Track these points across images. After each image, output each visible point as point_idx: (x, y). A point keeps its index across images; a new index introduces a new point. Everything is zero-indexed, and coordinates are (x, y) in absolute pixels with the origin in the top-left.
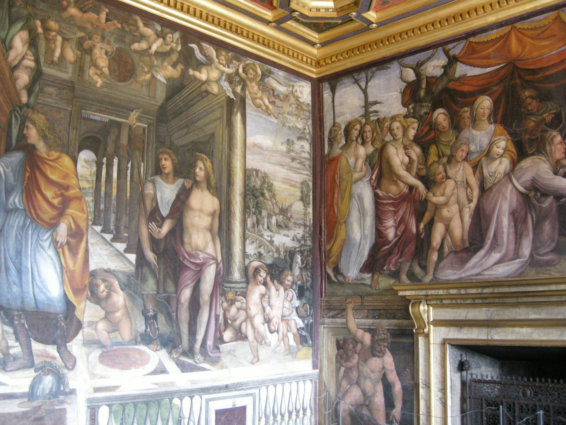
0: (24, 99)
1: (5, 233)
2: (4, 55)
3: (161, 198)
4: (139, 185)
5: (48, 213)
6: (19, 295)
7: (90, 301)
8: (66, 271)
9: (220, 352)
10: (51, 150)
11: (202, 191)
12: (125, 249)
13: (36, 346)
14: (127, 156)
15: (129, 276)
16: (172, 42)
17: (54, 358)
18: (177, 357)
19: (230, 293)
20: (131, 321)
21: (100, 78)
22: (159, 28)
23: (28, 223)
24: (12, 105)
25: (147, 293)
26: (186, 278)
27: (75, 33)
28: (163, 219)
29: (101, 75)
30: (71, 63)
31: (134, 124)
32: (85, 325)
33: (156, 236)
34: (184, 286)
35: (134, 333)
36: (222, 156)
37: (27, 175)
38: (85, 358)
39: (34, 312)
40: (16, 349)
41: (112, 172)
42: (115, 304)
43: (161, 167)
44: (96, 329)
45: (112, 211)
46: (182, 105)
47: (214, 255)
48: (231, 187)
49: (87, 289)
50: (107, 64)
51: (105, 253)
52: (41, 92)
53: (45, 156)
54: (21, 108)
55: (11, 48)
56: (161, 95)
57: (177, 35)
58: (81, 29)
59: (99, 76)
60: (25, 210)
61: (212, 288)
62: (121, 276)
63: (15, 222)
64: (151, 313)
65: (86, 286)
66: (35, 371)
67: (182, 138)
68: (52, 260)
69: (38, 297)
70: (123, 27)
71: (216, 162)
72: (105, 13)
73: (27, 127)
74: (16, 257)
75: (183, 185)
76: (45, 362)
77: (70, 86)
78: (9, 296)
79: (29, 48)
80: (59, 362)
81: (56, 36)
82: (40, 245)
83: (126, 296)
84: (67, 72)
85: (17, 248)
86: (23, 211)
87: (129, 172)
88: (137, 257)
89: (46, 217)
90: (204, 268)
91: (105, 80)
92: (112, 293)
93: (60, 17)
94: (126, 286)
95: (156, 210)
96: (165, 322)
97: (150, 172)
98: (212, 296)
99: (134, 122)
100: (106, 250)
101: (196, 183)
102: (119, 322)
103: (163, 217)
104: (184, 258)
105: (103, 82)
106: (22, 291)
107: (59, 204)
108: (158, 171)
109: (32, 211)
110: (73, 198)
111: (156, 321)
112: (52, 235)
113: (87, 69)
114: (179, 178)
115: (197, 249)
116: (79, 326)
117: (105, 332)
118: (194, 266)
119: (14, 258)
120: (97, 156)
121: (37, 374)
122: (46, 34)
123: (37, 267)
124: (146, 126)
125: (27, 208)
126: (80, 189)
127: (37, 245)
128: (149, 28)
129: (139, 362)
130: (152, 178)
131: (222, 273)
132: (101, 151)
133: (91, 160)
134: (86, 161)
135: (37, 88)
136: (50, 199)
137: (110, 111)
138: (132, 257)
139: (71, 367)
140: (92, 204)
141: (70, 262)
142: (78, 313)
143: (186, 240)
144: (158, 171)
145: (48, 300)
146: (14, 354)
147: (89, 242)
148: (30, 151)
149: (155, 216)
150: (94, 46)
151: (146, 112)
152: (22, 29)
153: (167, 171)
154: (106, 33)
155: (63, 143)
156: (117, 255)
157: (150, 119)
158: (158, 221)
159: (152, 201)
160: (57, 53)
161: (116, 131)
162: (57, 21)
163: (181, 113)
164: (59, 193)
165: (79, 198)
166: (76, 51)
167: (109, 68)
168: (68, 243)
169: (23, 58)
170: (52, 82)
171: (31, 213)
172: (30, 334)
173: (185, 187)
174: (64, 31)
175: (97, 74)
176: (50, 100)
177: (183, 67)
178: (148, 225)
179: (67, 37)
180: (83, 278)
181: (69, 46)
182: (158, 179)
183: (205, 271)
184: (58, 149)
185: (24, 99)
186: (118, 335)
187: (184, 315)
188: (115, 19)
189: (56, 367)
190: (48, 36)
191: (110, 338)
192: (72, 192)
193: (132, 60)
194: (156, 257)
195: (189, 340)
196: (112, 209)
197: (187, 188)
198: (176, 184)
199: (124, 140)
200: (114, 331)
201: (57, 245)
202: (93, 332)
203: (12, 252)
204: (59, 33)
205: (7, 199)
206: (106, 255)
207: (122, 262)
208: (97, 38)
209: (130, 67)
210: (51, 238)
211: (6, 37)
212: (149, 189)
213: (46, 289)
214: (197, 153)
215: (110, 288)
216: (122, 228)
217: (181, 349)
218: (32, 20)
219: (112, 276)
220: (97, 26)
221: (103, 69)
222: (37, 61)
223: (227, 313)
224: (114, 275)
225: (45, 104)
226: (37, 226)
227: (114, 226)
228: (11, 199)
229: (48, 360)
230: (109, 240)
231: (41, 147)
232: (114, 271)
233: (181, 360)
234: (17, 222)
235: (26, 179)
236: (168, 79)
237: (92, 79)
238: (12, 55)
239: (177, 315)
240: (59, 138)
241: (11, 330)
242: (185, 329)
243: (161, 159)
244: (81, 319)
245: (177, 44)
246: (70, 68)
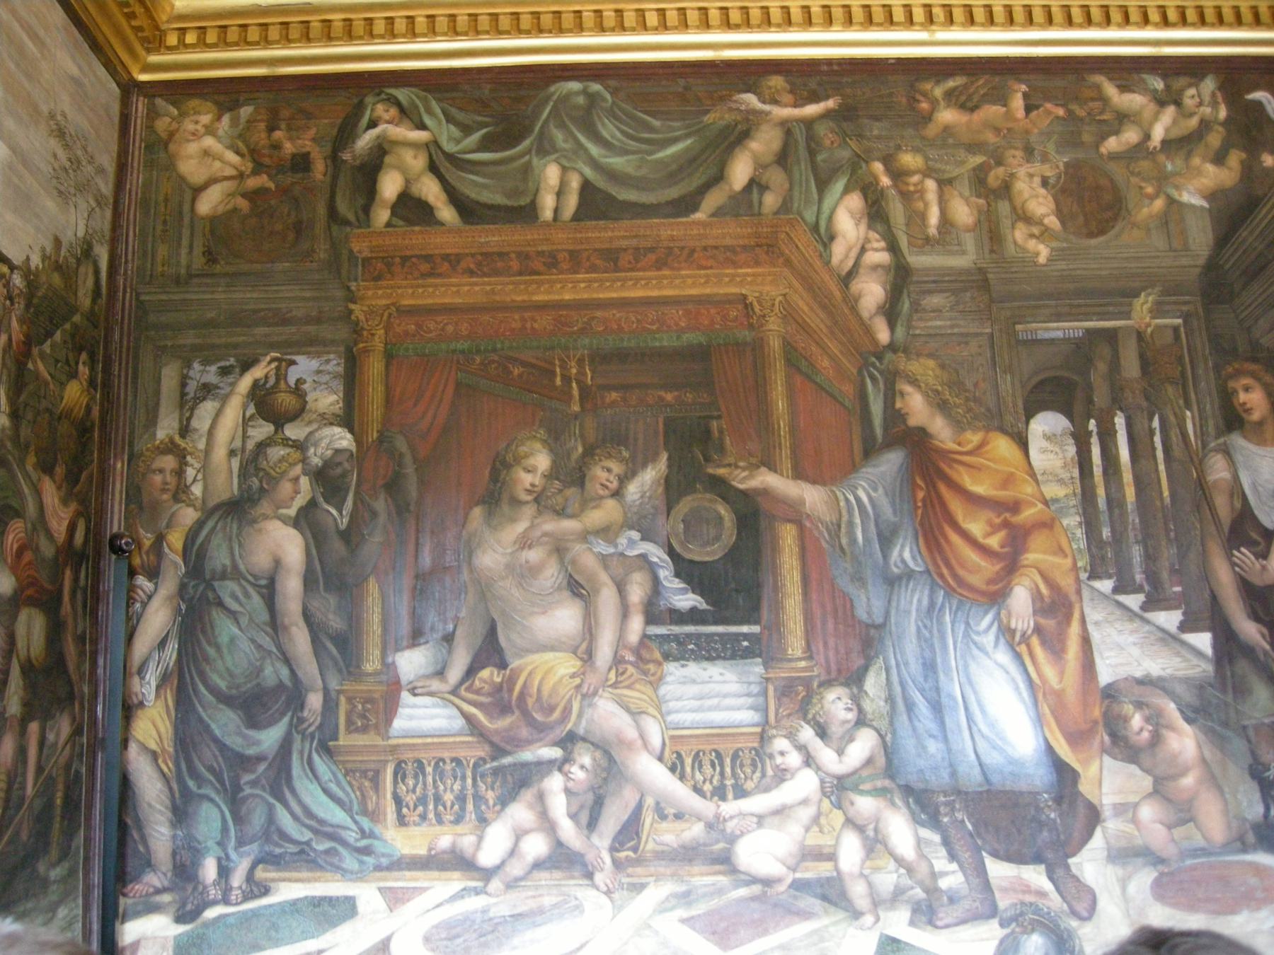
0: (883, 336)
1: (893, 628)
2: (821, 256)
3: (1254, 486)
4: (1188, 468)
5: (980, 569)
6: (943, 759)
7: (1110, 755)
8: (1044, 694)
10: (964, 430)
13: (998, 870)
14: (1145, 404)
15: (1200, 687)
16: (1201, 104)
17: (1042, 894)
21: (1043, 242)
22: (1159, 85)
23: (940, 599)
24: (861, 355)
25: (1254, 722)
27: (963, 163)
29: (1044, 234)
30: (968, 230)
31: (1148, 325)
32: (1107, 812)
33: (1257, 581)
35: (1235, 824)
37: (921, 495)
38: (1118, 891)
39: (981, 793)
40: (953, 879)
41: (1117, 449)
42: (1175, 756)
43: (1240, 409)
44: (1135, 821)
45: (1132, 539)
46: (1261, 247)
49: (1101, 728)
50: (1052, 206)
51: (1131, 639)
52: (917, 311)
53: (952, 446)
54: (880, 358)
55: (832, 238)
56: (1201, 238)
57: (1209, 85)
58: (974, 148)
59: (1037, 238)
60: (928, 571)
62: (1180, 689)
63: (911, 602)
65: (1096, 722)
66: (1002, 925)
68: (1007, 673)
69: (987, 760)
70: (1070, 113)
72: (1019, 95)
73: (902, 394)
74: (926, 678)
76: (1023, 903)
77: (978, 281)
78: (922, 763)
79: (870, 227)
80: (1055, 901)
81: (922, 182)
82: (975, 643)
83: (1202, 737)
84: (964, 253)
85: (923, 658)
86: (925, 576)
87: (1157, 439)
89: (976, 580)
91: (1055, 244)
93: (923, 138)
94: (1196, 711)
97: (1211, 429)
99: (1148, 320)
100: (1132, 632)
105: (1052, 249)
106: (949, 750)
107: (1002, 547)
108: (1233, 420)
109: (945, 571)
110: (1033, 526)
112: (998, 616)
113: (1008, 231)
116: (1094, 816)
117: (1159, 826)
119: (922, 680)
120: (1072, 421)
121: (1007, 931)
122: (900, 184)
123: (975, 692)
124: (1180, 321)
125: (931, 568)
126: (1046, 503)
127: (967, 644)
128: (1134, 92)
130: (1221, 440)
132: (1078, 407)
133: (1059, 431)
134: (1048, 437)
135: (907, 305)
136: (981, 540)
137: (1083, 310)
138: (1203, 641)
139: (1085, 914)
140: (1079, 533)
141: (1050, 672)
142: (1085, 787)
144: (1233, 420)
145: (1010, 763)
146: (950, 889)
147: (1088, 619)
148: (916, 443)
150: (1012, 175)
151: (1172, 290)
152: (846, 191)
153: (1256, 416)
154: (1033, 139)
155: (988, 410)
156: (1162, 640)
157: (1185, 303)
158: (1256, 543)
159: (1232, 496)
160: (934, 218)
161: (1106, 351)
162: (916, 150)
163: (1262, 268)
164: (998, 521)
165: (1047, 525)
166: (973, 199)
167: (1059, 213)
168: (1038, 630)
169: (863, 250)
170: (934, 282)
171: (942, 576)
172: (979, 842)
174: (938, 166)
175: (1032, 236)
176: (939, 323)
177: (1244, 155)
178: (1229, 556)
179: (946, 176)
180: (1085, 705)
181: (956, 193)
182: (1238, 441)
184: (977, 423)
185: (883, 336)
186: (1195, 830)
188: (1048, 99)
189: (1049, 913)
190: (904, 188)
191: (1173, 840)
192: (1028, 514)
193: (1112, 181)
194: (1265, 631)
196: (1131, 534)
199: (1131, 367)
200: (1183, 822)
201: (1013, 638)
202: (1130, 828)
203: (915, 667)
204: (928, 173)
205: (886, 557)
206: (1135, 644)
207: (1178, 654)
208: (1014, 157)
209: (1107, 197)
210: (996, 624)
211: (817, 217)
212: (1218, 470)
213: (1003, 739)
215: (1156, 721)
216: (1165, 575)
218: (864, 165)
220: (1009, 130)
221: (1046, 221)
222: (893, 247)
224: (1164, 689)
225: (930, 335)
226: (961, 603)
227: (1144, 572)
228: (895, 554)
229: (1029, 898)
231: (940, 429)
232: (1161, 679)
234: (915, 601)
235: (920, 504)
236: (1211, 196)
237: (1025, 250)
238: (838, 251)
240: (976, 400)
241: (936, 838)
243: (1235, 391)
244: (1095, 801)
245: (1214, 104)
246: (969, 241)
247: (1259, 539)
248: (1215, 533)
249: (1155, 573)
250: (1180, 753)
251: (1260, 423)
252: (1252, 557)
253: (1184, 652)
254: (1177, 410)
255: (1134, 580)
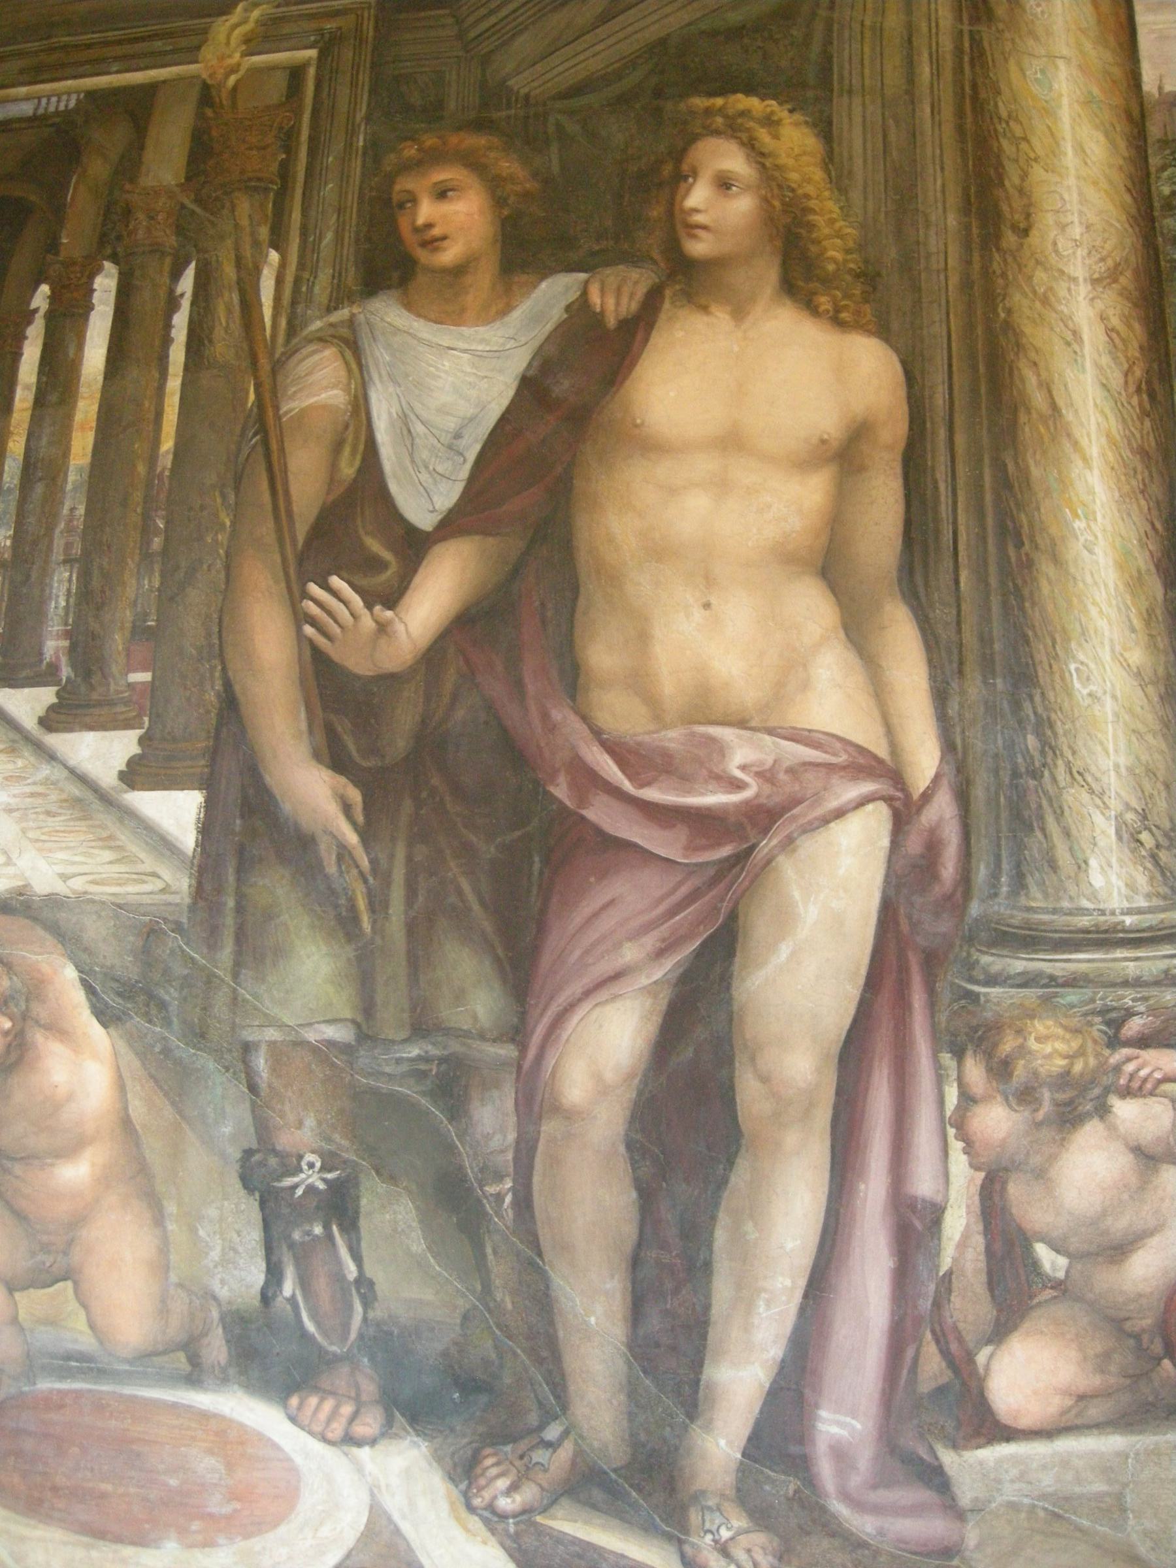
9: (960, 1515)
11: (739, 313)
12: (131, 762)
18: (527, 1511)
19: (1039, 1027)
20: (159, 1220)
25: (272, 1034)
26: (606, 923)
28: (414, 546)
31: (234, 70)
33: (356, 661)
34: (575, 988)
35: (179, 1304)
36: (910, 64)
41: (80, 347)
45: (58, 554)
47: (866, 733)
48: (1010, 239)
61: (852, 991)
62: (95, 930)
64: (311, 1177)
67: (569, 51)
71: (856, 120)
75: (580, 309)
83: (130, 1059)
87: (181, 320)
88: (210, 805)
90: (767, 845)
92: (38, 1037)
95: (363, 490)
96: (418, 1246)
98: (853, 1055)
101: (687, 279)
102: (78, 1221)
103: (411, 531)
104: (588, 781)
111: (350, 1225)
114: (546, 272)
115: (706, 708)
118: (681, 834)
124: (313, 53)
129: (216, 1505)
130: (343, 314)
131: (949, 870)
138: (178, 811)
143: (602, 655)
144: (388, 263)
149: (358, 534)
153: (449, 255)
156: (75, 803)
158: (377, 565)
159: (337, 447)
173: (598, 319)
178: (295, 597)
182: (387, 314)
183: (787, 867)
186: (73, 1305)
187: (591, 1202)
191: (14, 1321)
194: (355, 796)
195: (632, 1391)
196: (59, 543)
197: (611, 322)
198: (516, 314)
199: (165, 164)
200: (43, 1278)
206: (9, 810)
207: (108, 842)
212: (317, 385)
214: (699, 102)
216: (118, 641)
217: (565, 1453)
219: (40, 932)
223: (1015, 1190)
227: (68, 635)
230: (29, 722)
232: (54, 901)
233: (560, 1539)
239: (524, 1203)
242: (594, 1311)
243: (414, 200)
247: (387, 555)
248: (270, 538)
249: (94, 637)
250: (70, 1097)
251: (459, 271)
252: (357, 601)
253: (124, 838)
254: (247, 252)
255: (41, 654)
